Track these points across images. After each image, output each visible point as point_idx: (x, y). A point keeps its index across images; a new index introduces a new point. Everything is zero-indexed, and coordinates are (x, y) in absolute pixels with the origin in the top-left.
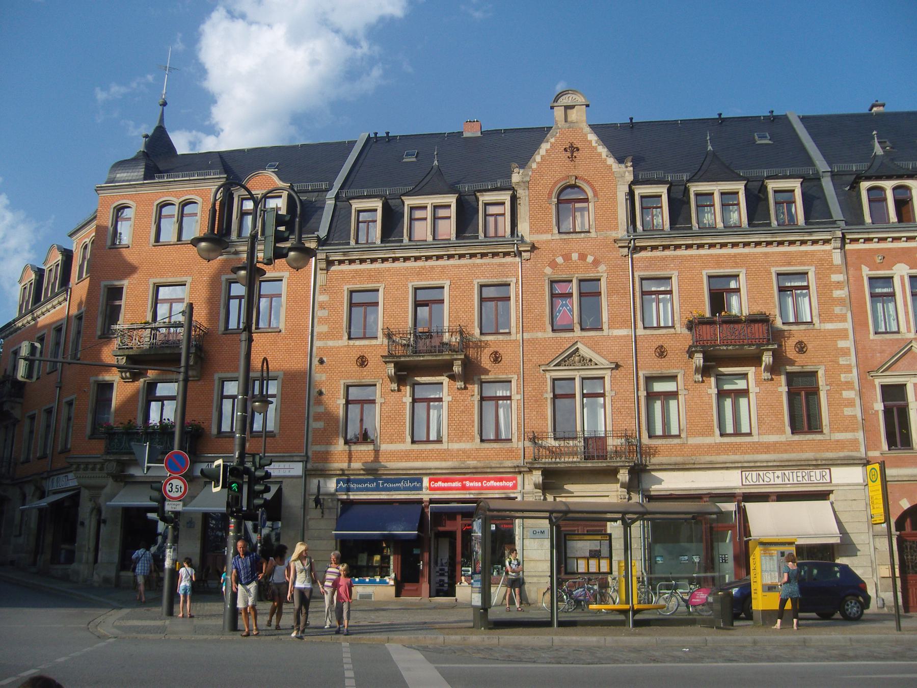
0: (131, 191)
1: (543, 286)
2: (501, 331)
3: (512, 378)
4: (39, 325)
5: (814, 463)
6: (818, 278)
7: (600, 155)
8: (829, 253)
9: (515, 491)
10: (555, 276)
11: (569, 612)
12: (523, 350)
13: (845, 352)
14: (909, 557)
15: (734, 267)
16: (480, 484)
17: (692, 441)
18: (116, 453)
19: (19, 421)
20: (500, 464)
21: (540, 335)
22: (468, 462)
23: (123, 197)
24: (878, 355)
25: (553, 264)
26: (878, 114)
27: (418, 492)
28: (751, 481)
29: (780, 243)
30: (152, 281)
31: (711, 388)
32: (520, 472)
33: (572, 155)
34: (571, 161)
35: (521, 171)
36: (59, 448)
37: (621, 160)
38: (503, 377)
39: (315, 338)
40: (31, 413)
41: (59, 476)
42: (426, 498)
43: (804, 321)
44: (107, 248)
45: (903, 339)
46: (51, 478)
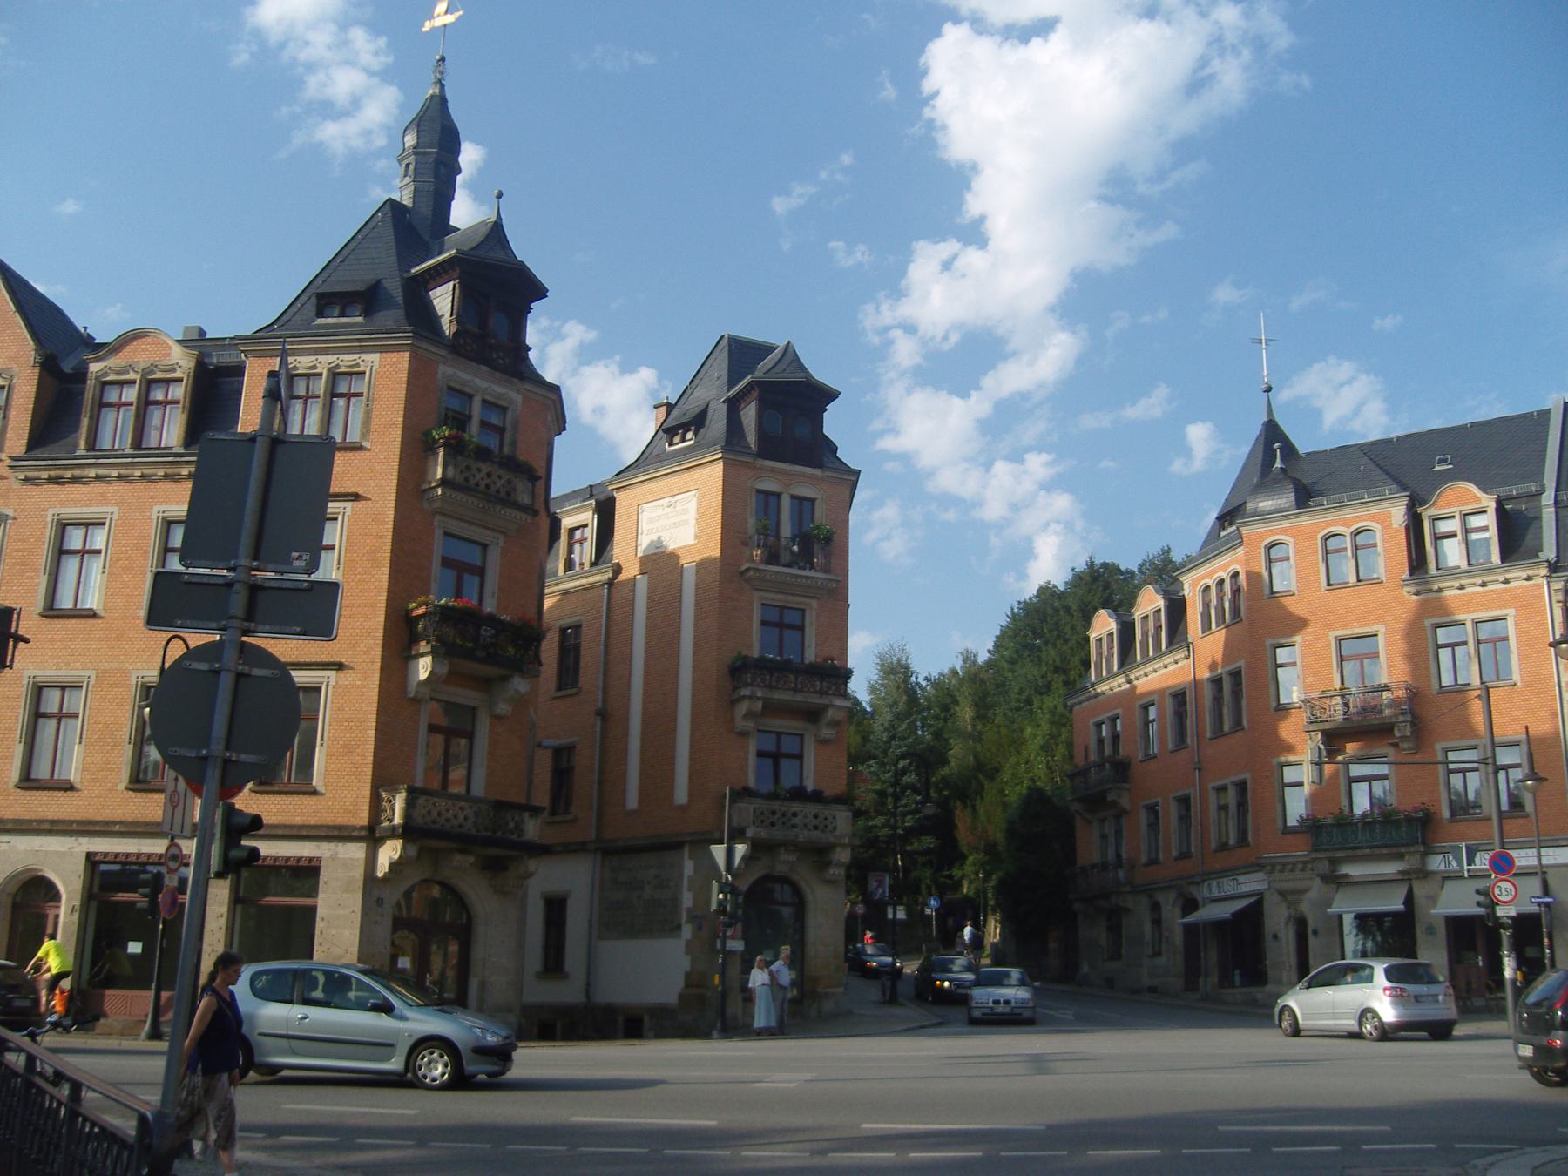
0: (1285, 524)
4: (1138, 691)
18: (1327, 850)
19: (1127, 812)
23: (1274, 532)
30: (1333, 634)
36: (1213, 845)
39: (1564, 689)
40: (1148, 802)
41: (1221, 880)
44: (1265, 597)
46: (1206, 883)
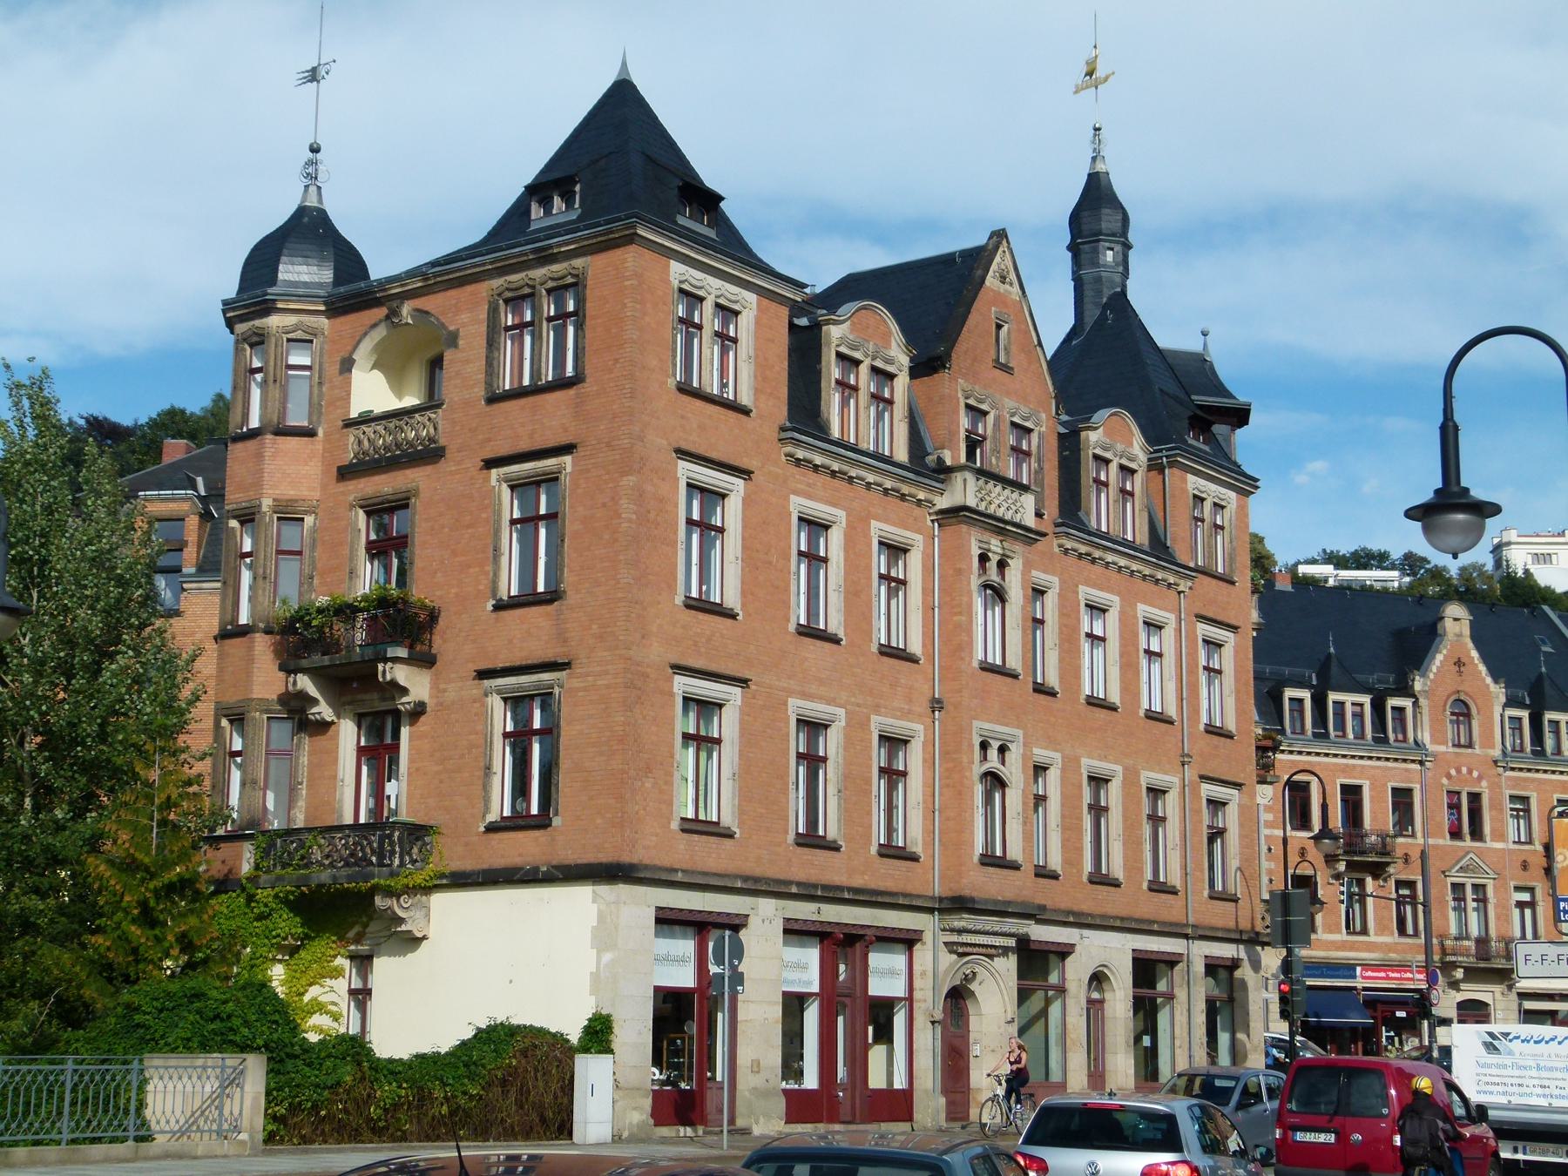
37: (1496, 681)
42: (1359, 986)
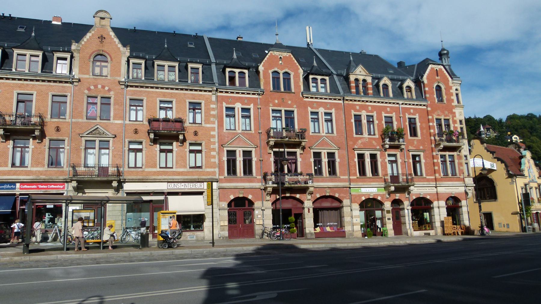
1: (83, 99)
2: (61, 117)
3: (65, 139)
5: (197, 180)
6: (205, 106)
7: (115, 42)
8: (211, 96)
9: (64, 190)
10: (90, 94)
11: (70, 245)
12: (72, 127)
13: (213, 136)
14: (232, 218)
15: (171, 98)
16: (46, 187)
17: (147, 170)
20: (57, 178)
21: (80, 120)
22: (41, 177)
24: (227, 138)
25: (89, 89)
26: (240, 41)
27: (13, 190)
28: (171, 187)
29: (191, 90)
31: (157, 148)
32: (67, 182)
33: (102, 41)
34: (101, 43)
35: (76, 44)
37: (124, 46)
38: (61, 138)
42: (18, 193)
43: (131, 120)
45: (236, 133)
